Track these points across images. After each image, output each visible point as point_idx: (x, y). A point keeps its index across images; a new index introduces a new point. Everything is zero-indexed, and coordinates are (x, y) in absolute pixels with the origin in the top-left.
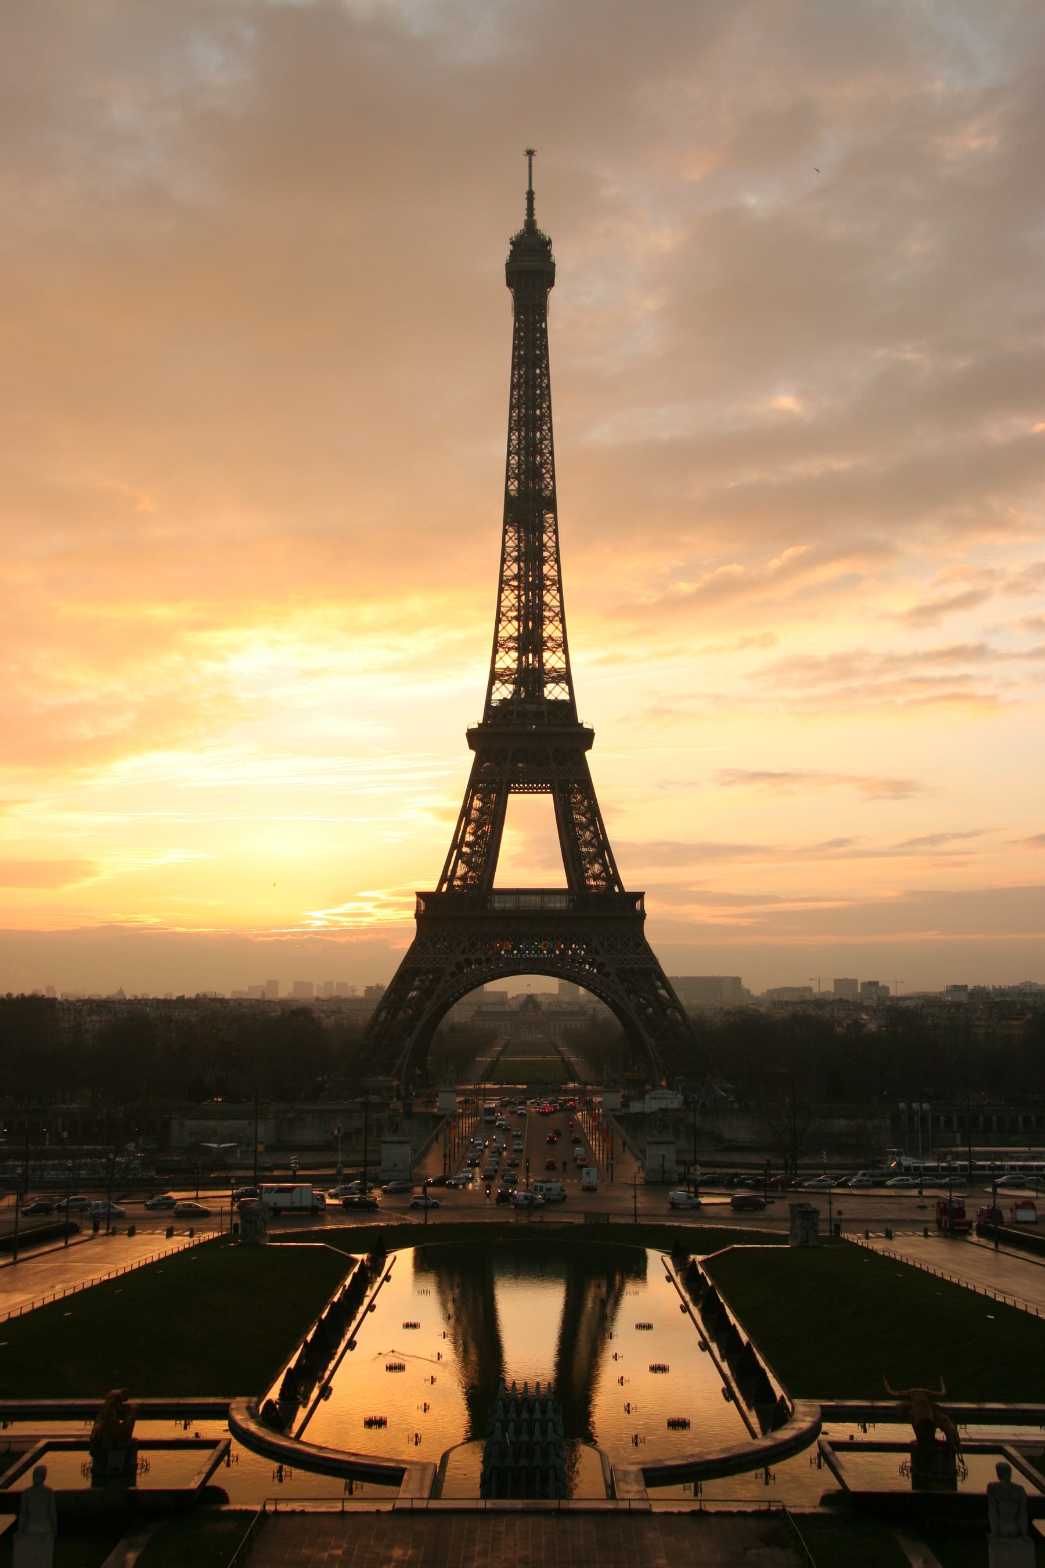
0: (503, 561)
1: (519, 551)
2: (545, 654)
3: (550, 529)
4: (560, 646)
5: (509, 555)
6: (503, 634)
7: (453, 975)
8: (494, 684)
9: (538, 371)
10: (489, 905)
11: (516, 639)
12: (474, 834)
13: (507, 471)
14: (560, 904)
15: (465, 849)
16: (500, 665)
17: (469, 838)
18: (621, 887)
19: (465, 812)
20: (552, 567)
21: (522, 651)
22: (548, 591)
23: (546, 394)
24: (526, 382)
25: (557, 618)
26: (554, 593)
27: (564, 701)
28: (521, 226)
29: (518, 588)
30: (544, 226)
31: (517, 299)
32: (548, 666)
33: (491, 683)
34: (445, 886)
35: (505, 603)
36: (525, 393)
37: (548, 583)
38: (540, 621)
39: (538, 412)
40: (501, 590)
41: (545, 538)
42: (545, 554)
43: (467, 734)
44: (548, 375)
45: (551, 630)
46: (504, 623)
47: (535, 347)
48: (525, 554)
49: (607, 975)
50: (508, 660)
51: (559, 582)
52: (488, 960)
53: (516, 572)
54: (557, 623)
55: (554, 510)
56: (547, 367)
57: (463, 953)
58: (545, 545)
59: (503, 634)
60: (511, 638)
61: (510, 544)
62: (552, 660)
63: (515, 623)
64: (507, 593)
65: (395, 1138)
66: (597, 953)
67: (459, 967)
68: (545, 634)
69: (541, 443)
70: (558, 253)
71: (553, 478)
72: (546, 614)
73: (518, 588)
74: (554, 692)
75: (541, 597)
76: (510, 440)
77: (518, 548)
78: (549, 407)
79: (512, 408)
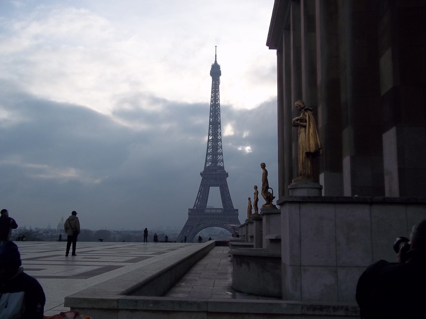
0: (209, 136)
4: (220, 155)
6: (209, 152)
7: (196, 227)
14: (220, 211)
16: (208, 158)
29: (212, 141)
30: (218, 63)
35: (210, 145)
38: (217, 149)
59: (209, 152)
62: (220, 157)
67: (197, 225)
69: (218, 109)
73: (212, 141)
75: (217, 144)
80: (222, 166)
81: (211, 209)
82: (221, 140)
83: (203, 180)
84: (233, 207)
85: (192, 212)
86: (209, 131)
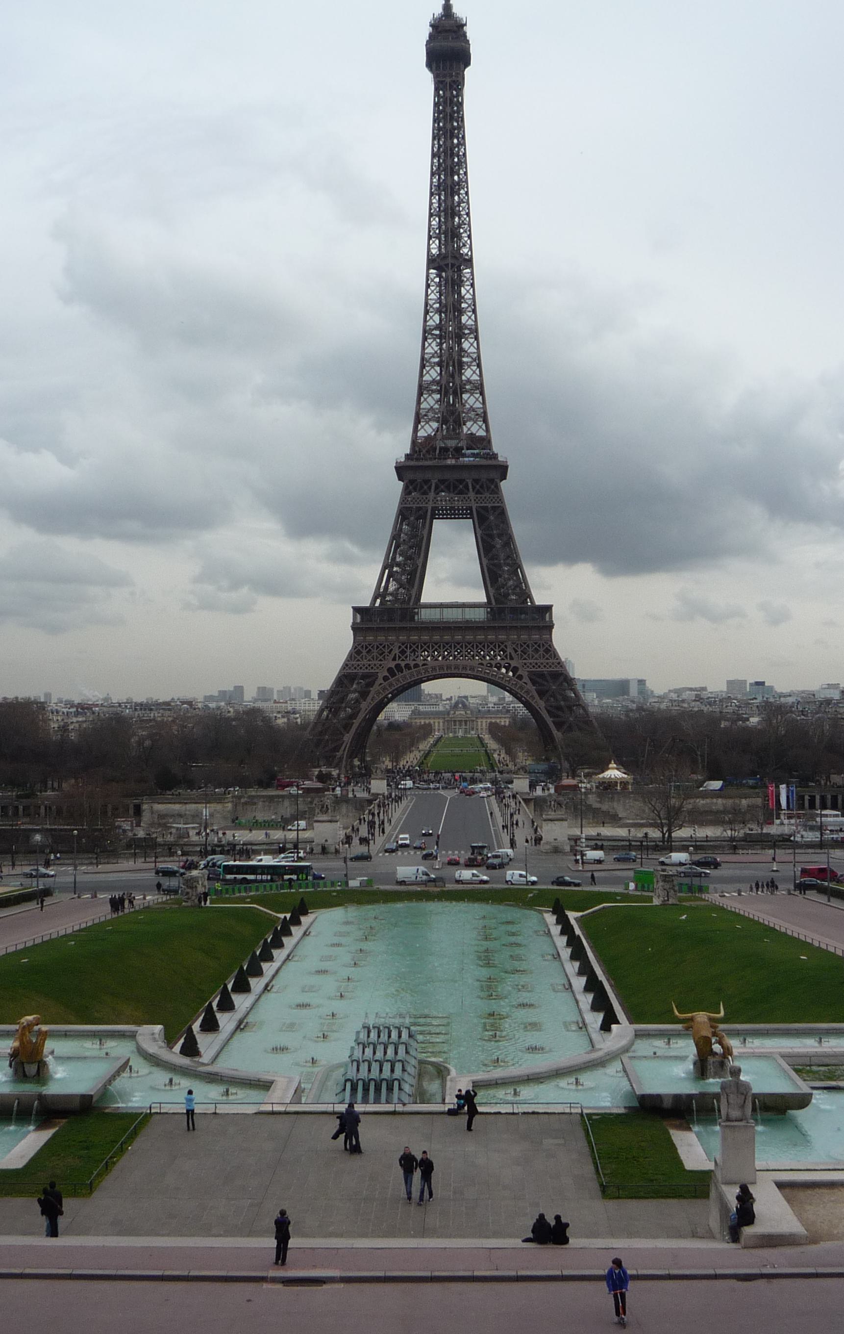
0: (427, 312)
1: (440, 303)
2: (464, 395)
3: (468, 283)
5: (431, 307)
6: (427, 378)
7: (385, 679)
8: (419, 422)
9: (455, 141)
10: (416, 618)
11: (438, 383)
12: (400, 555)
13: (429, 231)
14: (480, 615)
15: (395, 569)
16: (424, 405)
17: (399, 559)
18: (532, 601)
19: (395, 537)
20: (470, 317)
21: (444, 391)
22: (466, 339)
23: (462, 162)
24: (445, 152)
25: (474, 363)
26: (472, 340)
27: (481, 437)
28: (439, 10)
29: (440, 337)
30: (458, 10)
31: (436, 77)
32: (468, 406)
33: (417, 421)
34: (378, 601)
36: (444, 160)
37: (467, 331)
39: (456, 178)
40: (425, 339)
41: (463, 291)
42: (464, 305)
43: (396, 468)
44: (464, 144)
45: (469, 374)
46: (428, 368)
47: (452, 119)
48: (446, 306)
49: (520, 677)
50: (431, 401)
51: (476, 331)
52: (416, 666)
53: (438, 322)
54: (474, 368)
55: (471, 267)
56: (463, 137)
57: (394, 659)
58: (463, 298)
59: (427, 378)
60: (434, 382)
61: (432, 296)
62: (471, 400)
63: (438, 369)
64: (430, 341)
65: (325, 817)
66: (512, 658)
67: (390, 670)
68: (464, 378)
69: (459, 206)
70: (471, 32)
71: (469, 237)
72: (465, 359)
73: (440, 337)
74: (474, 428)
75: (460, 344)
76: (431, 204)
77: (439, 301)
78: (466, 173)
79: (433, 174)
80: (482, 433)
81: (441, 606)
82: (475, 331)
83: (407, 491)
84: (530, 596)
85: (366, 620)
86: (427, 295)
